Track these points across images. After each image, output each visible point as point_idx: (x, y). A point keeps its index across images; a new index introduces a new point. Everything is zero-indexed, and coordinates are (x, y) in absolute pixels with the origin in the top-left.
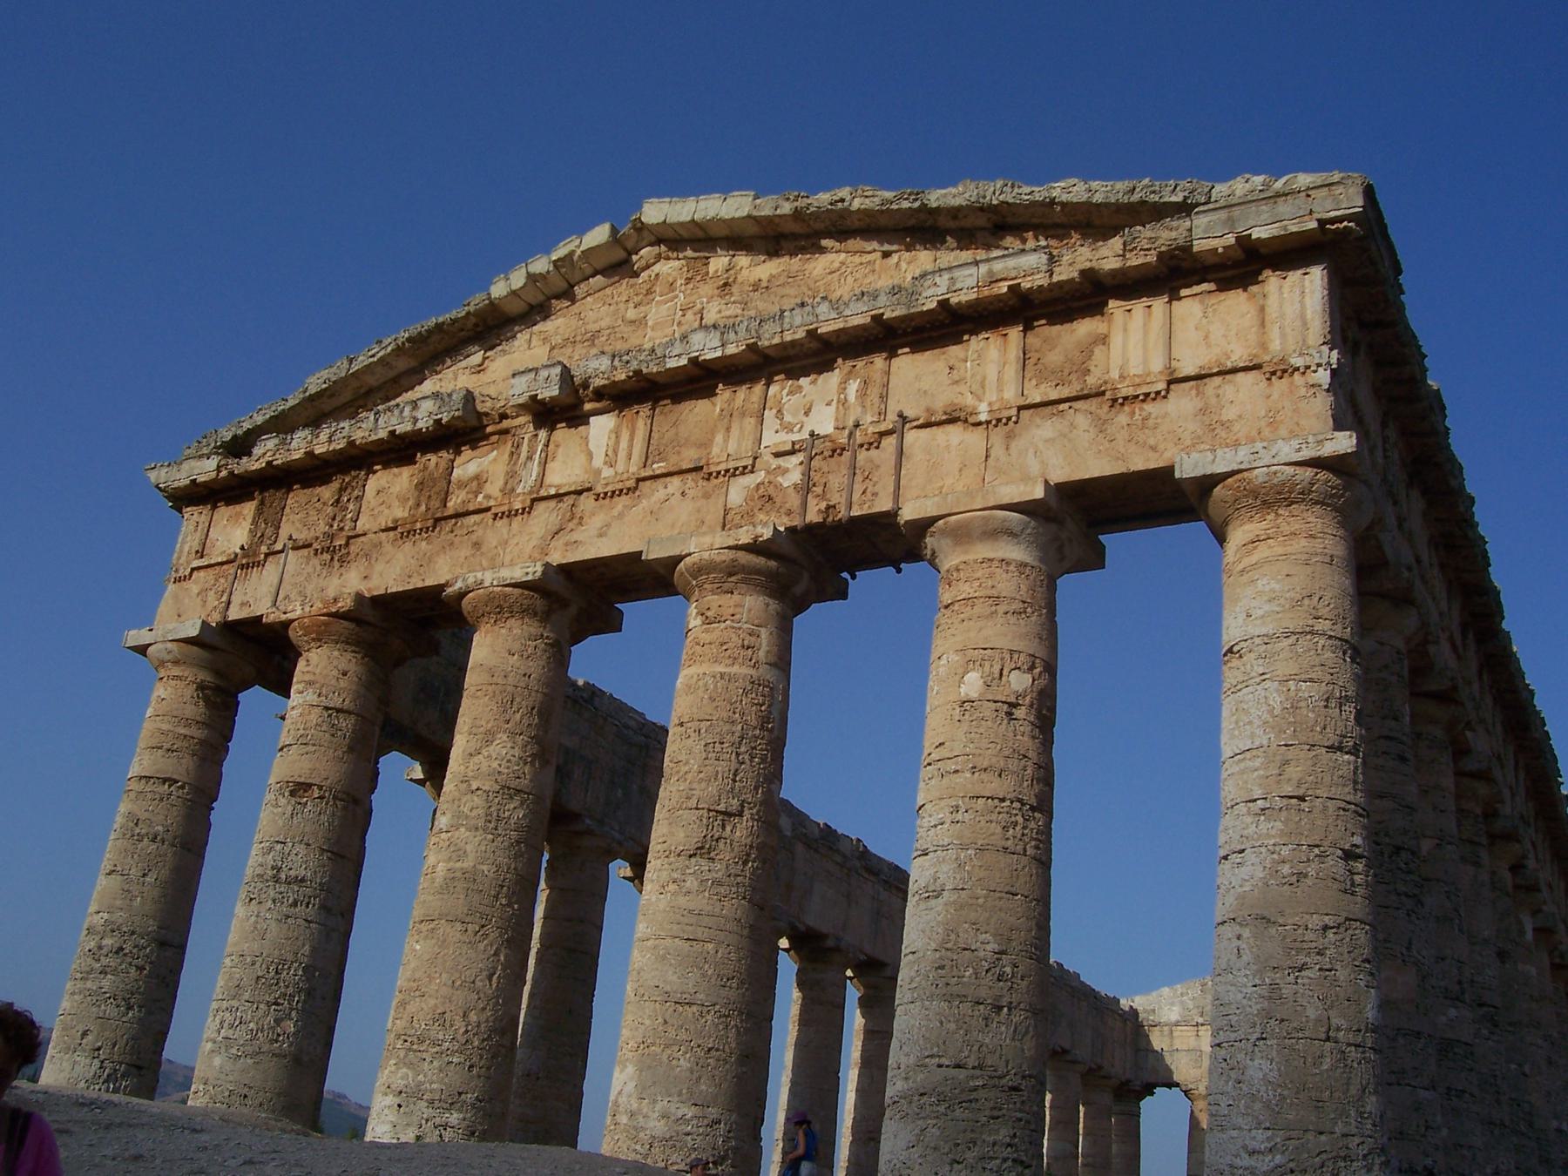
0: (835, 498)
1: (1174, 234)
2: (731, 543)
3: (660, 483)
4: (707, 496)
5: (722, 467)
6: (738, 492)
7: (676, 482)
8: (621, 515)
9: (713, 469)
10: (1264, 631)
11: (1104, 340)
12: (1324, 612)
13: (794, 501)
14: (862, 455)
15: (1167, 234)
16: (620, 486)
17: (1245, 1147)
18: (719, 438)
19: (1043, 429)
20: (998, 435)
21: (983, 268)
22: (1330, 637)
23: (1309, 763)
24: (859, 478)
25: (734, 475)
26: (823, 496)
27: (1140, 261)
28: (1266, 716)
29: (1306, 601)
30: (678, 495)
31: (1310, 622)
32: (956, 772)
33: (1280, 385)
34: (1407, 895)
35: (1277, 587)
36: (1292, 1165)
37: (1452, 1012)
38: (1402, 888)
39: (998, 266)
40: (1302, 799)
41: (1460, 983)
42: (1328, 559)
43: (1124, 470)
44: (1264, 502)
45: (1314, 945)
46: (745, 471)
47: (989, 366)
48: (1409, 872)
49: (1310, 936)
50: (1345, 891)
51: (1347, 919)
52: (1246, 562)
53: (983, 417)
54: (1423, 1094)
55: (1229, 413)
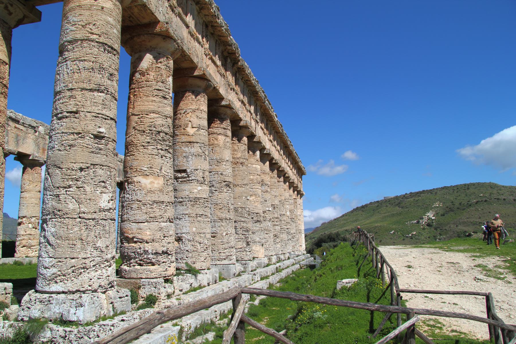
10: (68, 39)
12: (95, 31)
17: (43, 265)
22: (97, 42)
23: (80, 96)
28: (66, 76)
29: (88, 26)
31: (87, 35)
34: (162, 150)
35: (75, 19)
36: (59, 273)
37: (200, 188)
38: (159, 147)
40: (76, 112)
41: (203, 178)
42: (100, 8)
45: (74, 177)
48: (164, 140)
49: (74, 173)
50: (93, 152)
51: (91, 164)
54: (163, 224)
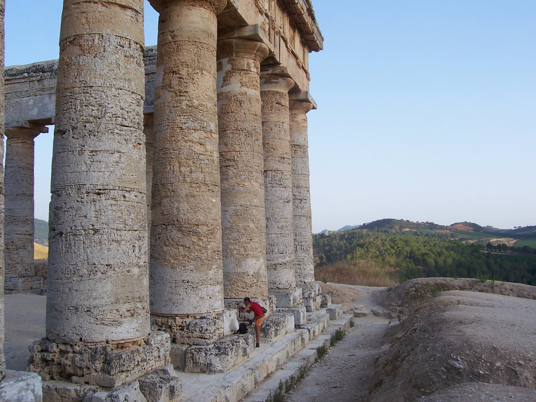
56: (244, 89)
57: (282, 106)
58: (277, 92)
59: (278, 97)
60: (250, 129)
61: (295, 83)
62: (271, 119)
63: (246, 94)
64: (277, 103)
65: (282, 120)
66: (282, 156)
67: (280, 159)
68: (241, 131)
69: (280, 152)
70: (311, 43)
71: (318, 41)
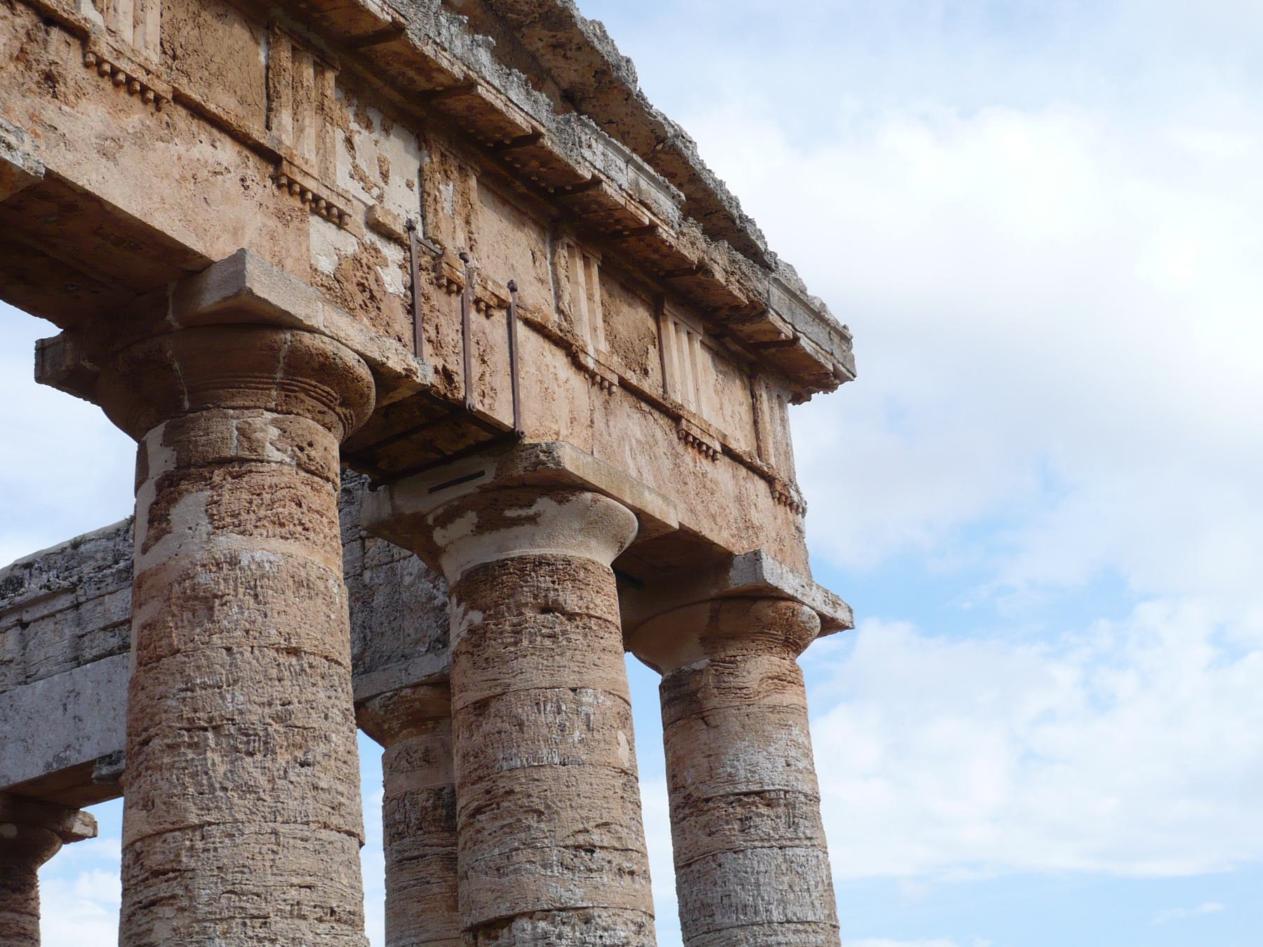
0: (454, 365)
1: (760, 288)
2: (376, 355)
3: (205, 133)
4: (280, 215)
5: (310, 184)
6: (325, 246)
7: (228, 152)
8: (139, 139)
9: (299, 178)
11: (658, 340)
13: (402, 324)
14: (473, 315)
15: (762, 285)
16: (141, 76)
18: (285, 117)
19: (632, 424)
20: (598, 398)
21: (632, 173)
24: (474, 350)
25: (315, 211)
26: (437, 345)
27: (736, 293)
30: (234, 177)
32: (632, 873)
33: (781, 510)
39: (644, 184)
43: (696, 528)
44: (787, 640)
46: (338, 219)
47: (583, 294)
52: (775, 699)
53: (591, 364)
55: (756, 517)
56: (228, 542)
57: (571, 616)
58: (540, 562)
59: (545, 582)
60: (255, 715)
61: (640, 514)
62: (518, 683)
63: (234, 562)
64: (545, 610)
65: (571, 679)
66: (581, 839)
67: (568, 855)
68: (210, 735)
69: (569, 819)
70: (779, 356)
71: (804, 342)
